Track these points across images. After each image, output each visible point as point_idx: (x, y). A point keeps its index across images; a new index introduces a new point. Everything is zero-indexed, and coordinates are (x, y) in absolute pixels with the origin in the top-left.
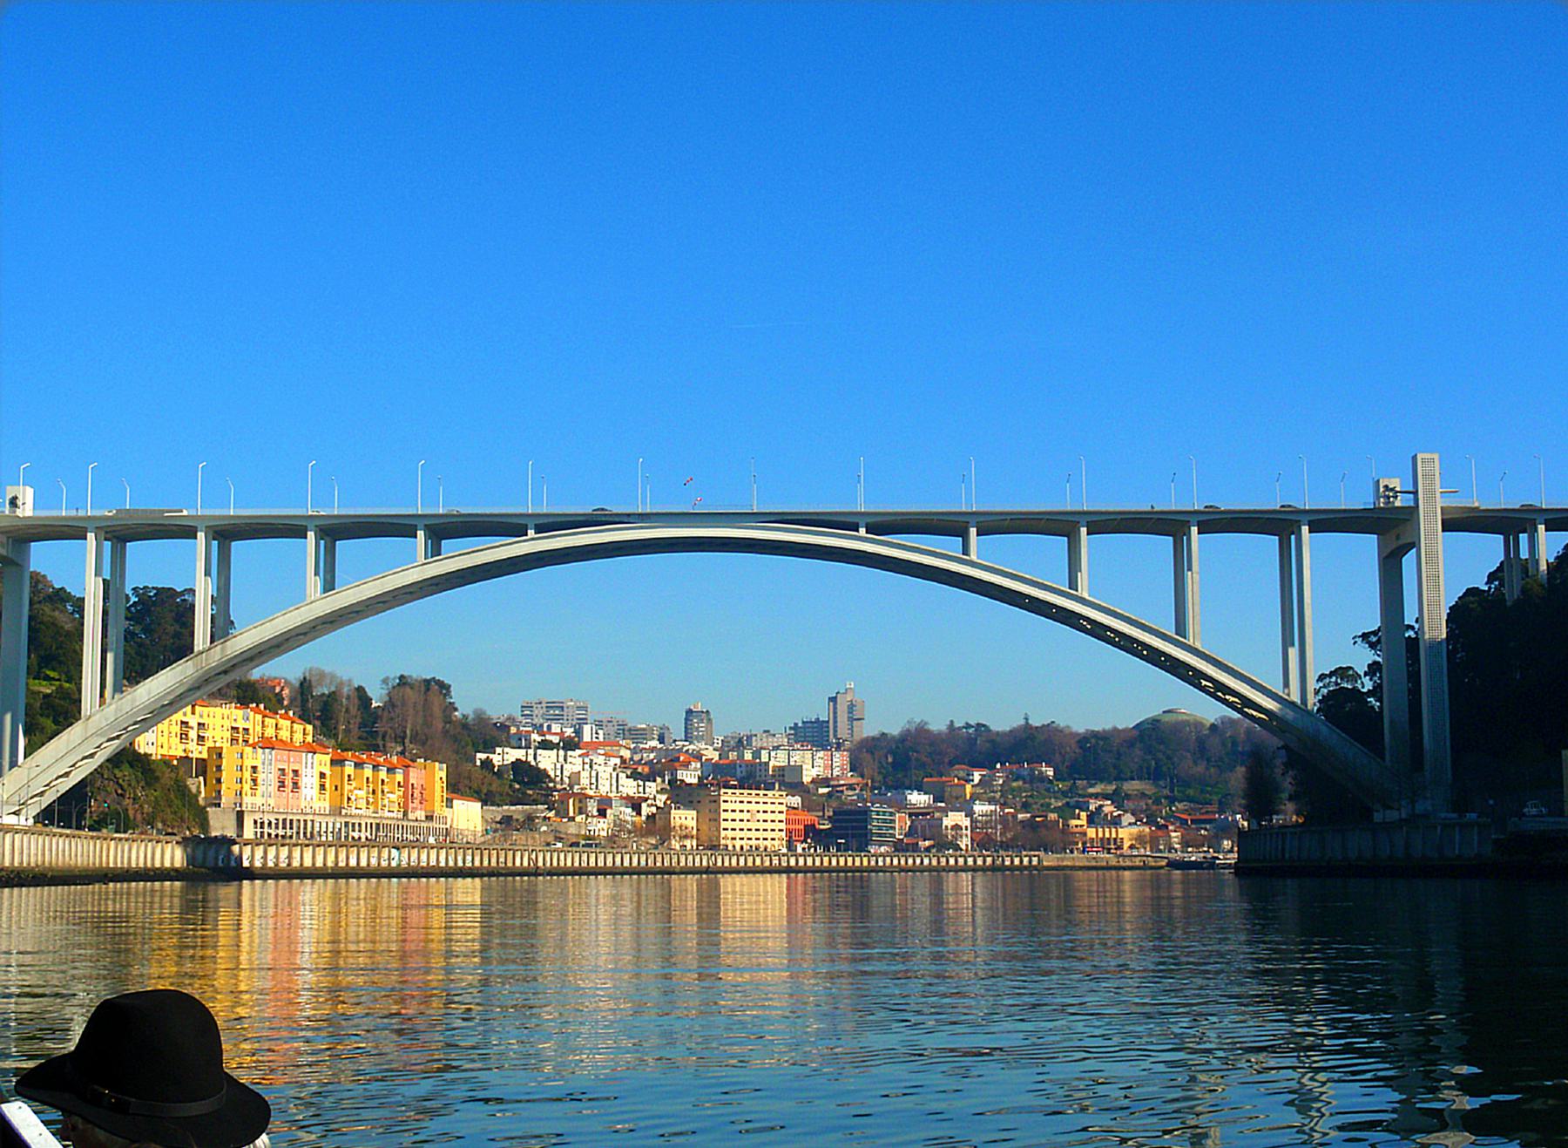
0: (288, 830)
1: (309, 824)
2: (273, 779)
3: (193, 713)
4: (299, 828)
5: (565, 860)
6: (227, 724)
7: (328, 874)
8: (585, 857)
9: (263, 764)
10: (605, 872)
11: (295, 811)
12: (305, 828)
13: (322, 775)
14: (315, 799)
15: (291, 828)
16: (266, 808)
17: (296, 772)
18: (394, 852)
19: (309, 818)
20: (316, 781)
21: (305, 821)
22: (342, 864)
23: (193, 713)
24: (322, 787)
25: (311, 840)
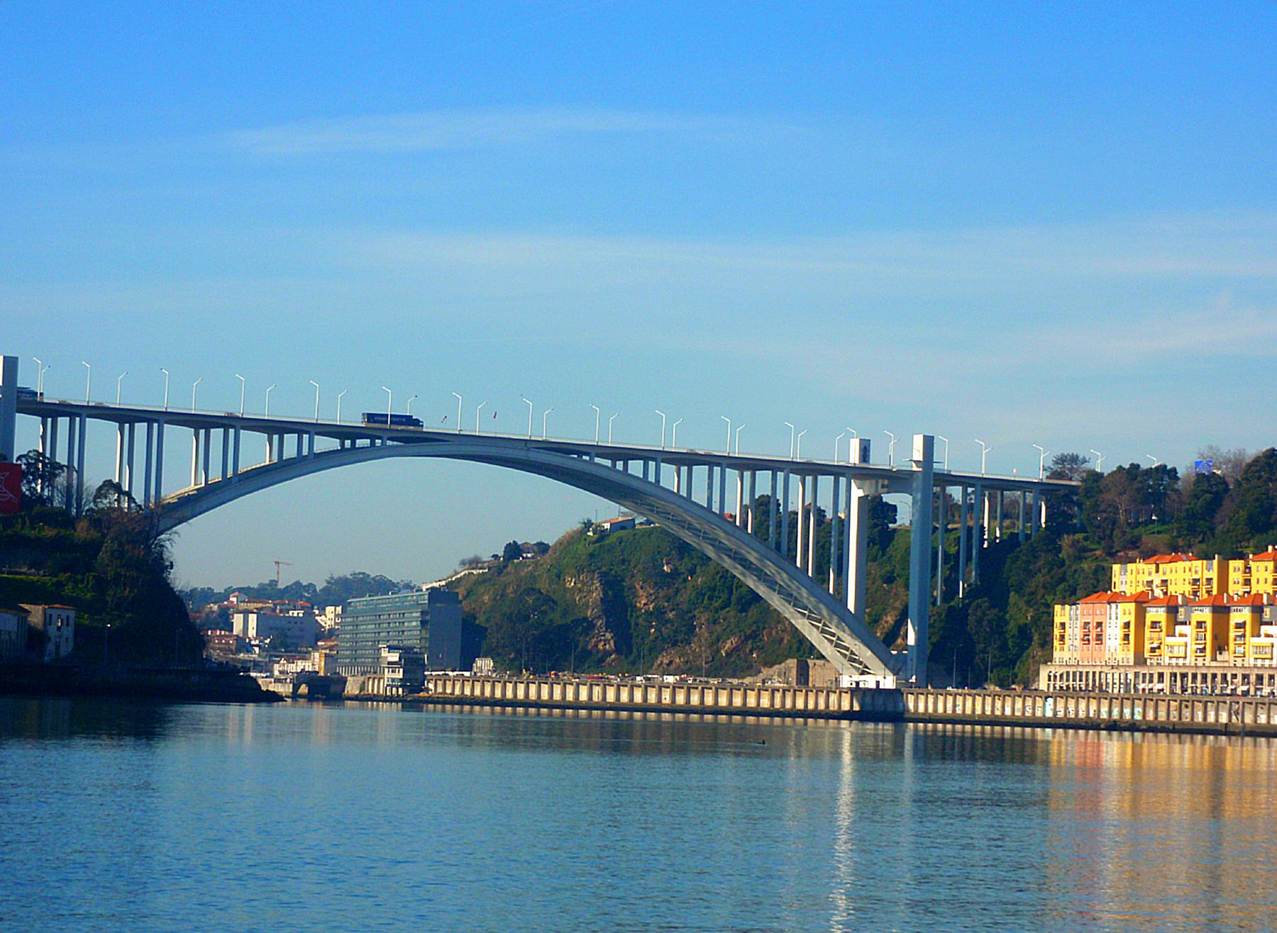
0: (1071, 683)
1: (1103, 676)
2: (1079, 633)
3: (1157, 571)
4: (1087, 680)
5: (1024, 707)
6: (1190, 576)
7: (977, 721)
8: (998, 704)
9: (1070, 619)
10: (1113, 726)
11: (1098, 663)
12: (1094, 681)
13: (1127, 625)
14: (1119, 649)
15: (1081, 680)
16: (1072, 662)
17: (1099, 624)
18: (1039, 702)
19: (1098, 670)
20: (1120, 633)
21: (1094, 673)
22: (1061, 714)
23: (1157, 571)
24: (1126, 637)
25: (1098, 691)
